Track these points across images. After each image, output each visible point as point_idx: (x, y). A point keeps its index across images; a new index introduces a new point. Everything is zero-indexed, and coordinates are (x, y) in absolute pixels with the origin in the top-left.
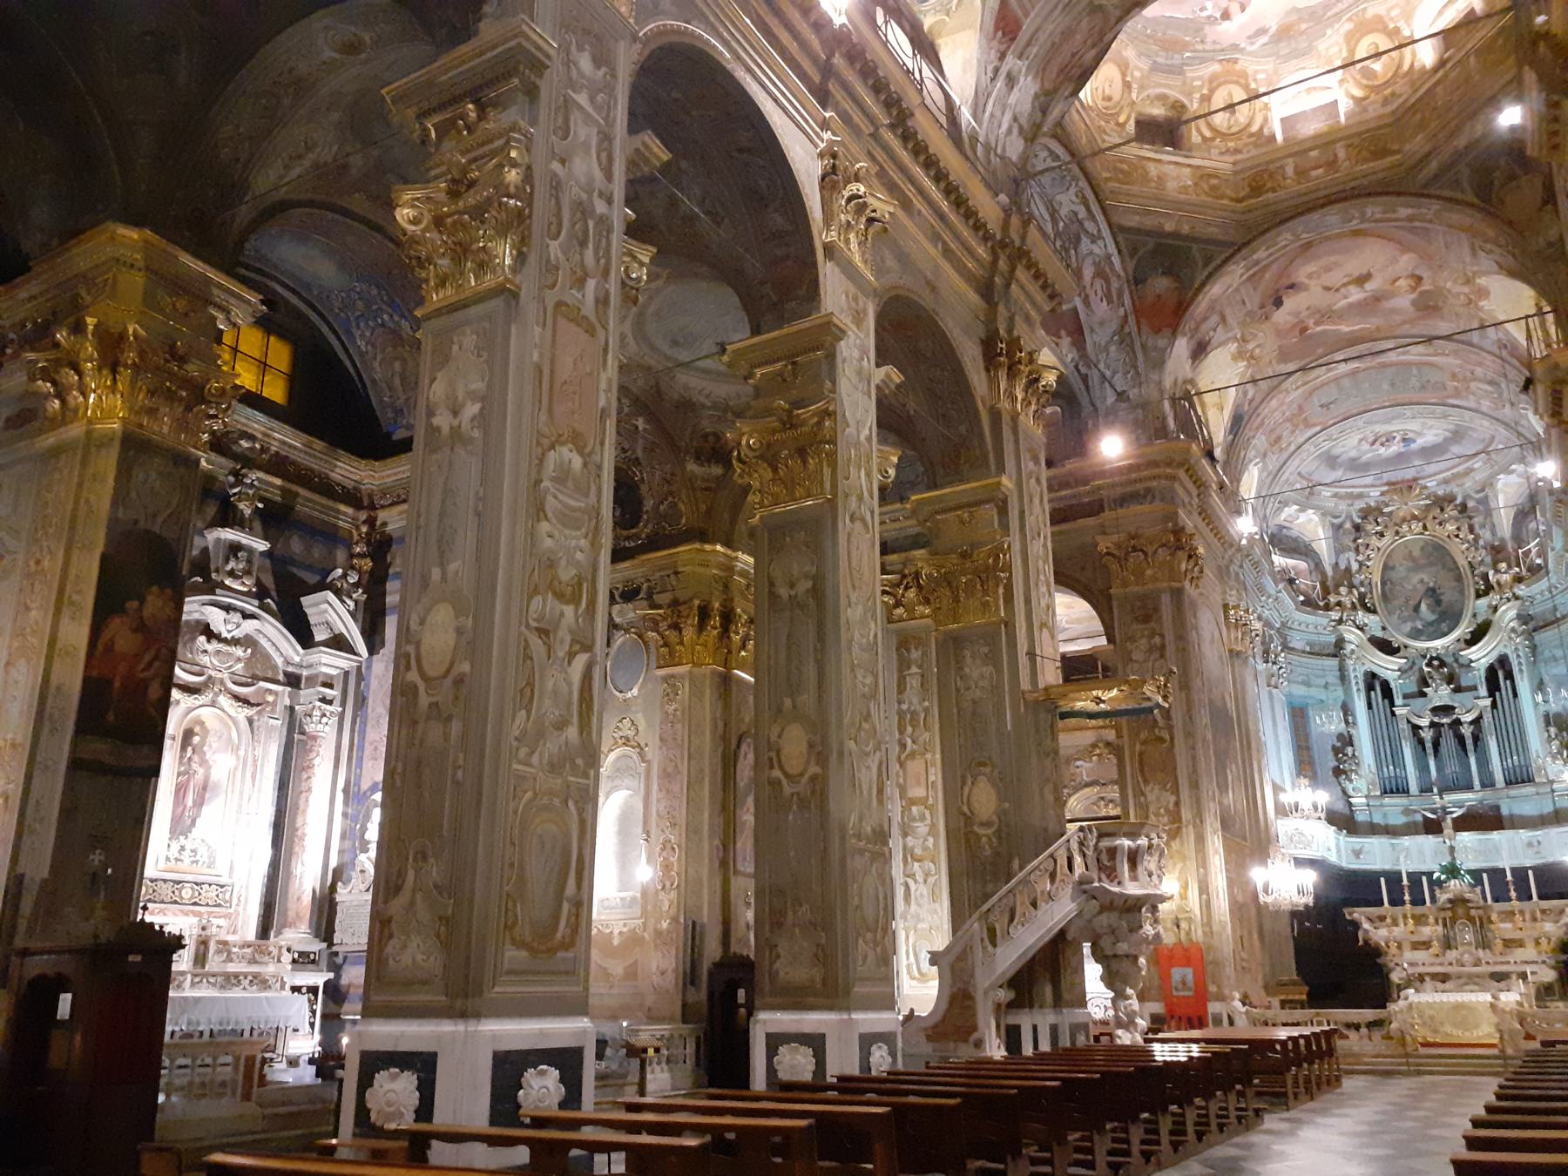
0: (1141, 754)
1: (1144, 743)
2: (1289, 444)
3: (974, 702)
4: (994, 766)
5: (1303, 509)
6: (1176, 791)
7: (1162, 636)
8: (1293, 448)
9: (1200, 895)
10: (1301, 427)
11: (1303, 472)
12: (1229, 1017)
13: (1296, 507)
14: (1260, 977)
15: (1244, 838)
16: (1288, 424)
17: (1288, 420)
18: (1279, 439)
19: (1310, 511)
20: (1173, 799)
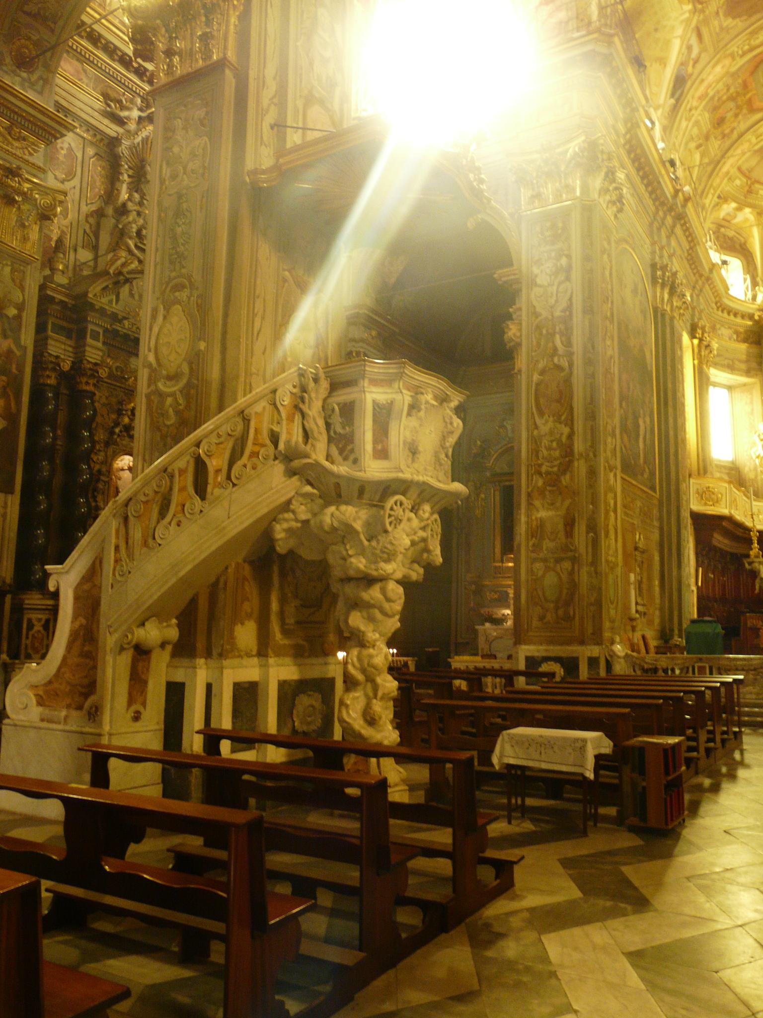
0: (537, 385)
1: (542, 372)
2: (732, 131)
3: (180, 196)
4: (192, 285)
5: (739, 209)
6: (570, 423)
7: (569, 257)
8: (735, 135)
9: (587, 533)
10: (745, 111)
11: (744, 168)
12: (607, 662)
13: (734, 205)
14: (657, 621)
15: (653, 488)
16: (731, 105)
17: (732, 98)
18: (720, 122)
19: (747, 210)
20: (566, 430)
